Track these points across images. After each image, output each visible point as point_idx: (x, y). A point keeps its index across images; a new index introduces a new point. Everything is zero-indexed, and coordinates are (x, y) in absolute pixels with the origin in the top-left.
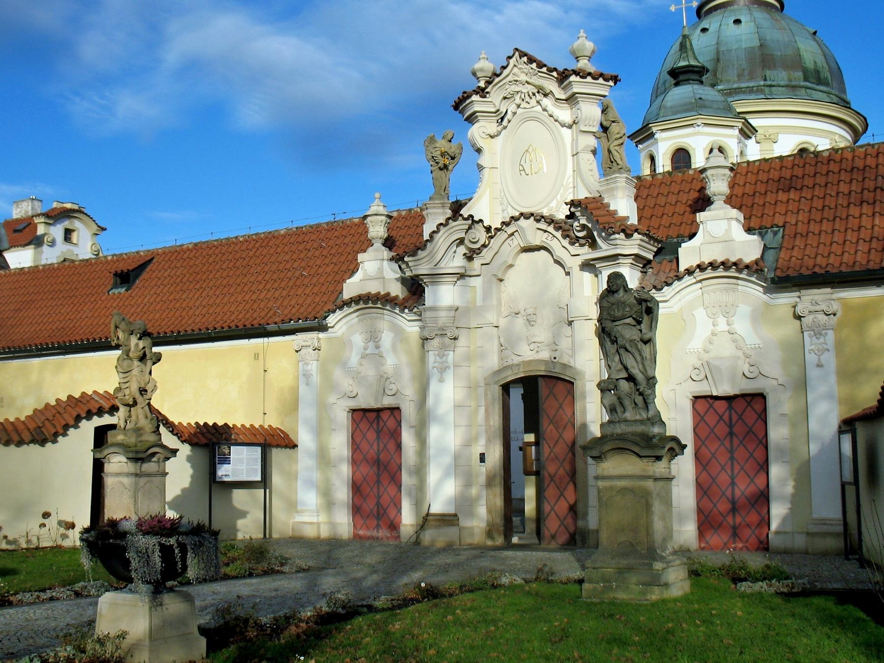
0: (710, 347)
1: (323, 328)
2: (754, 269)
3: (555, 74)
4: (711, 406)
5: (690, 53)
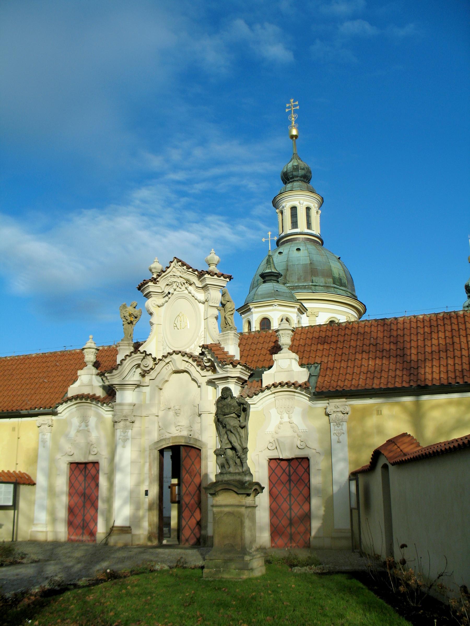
1: (55, 414)
2: (304, 387)
3: (196, 273)
4: (279, 464)
5: (272, 265)
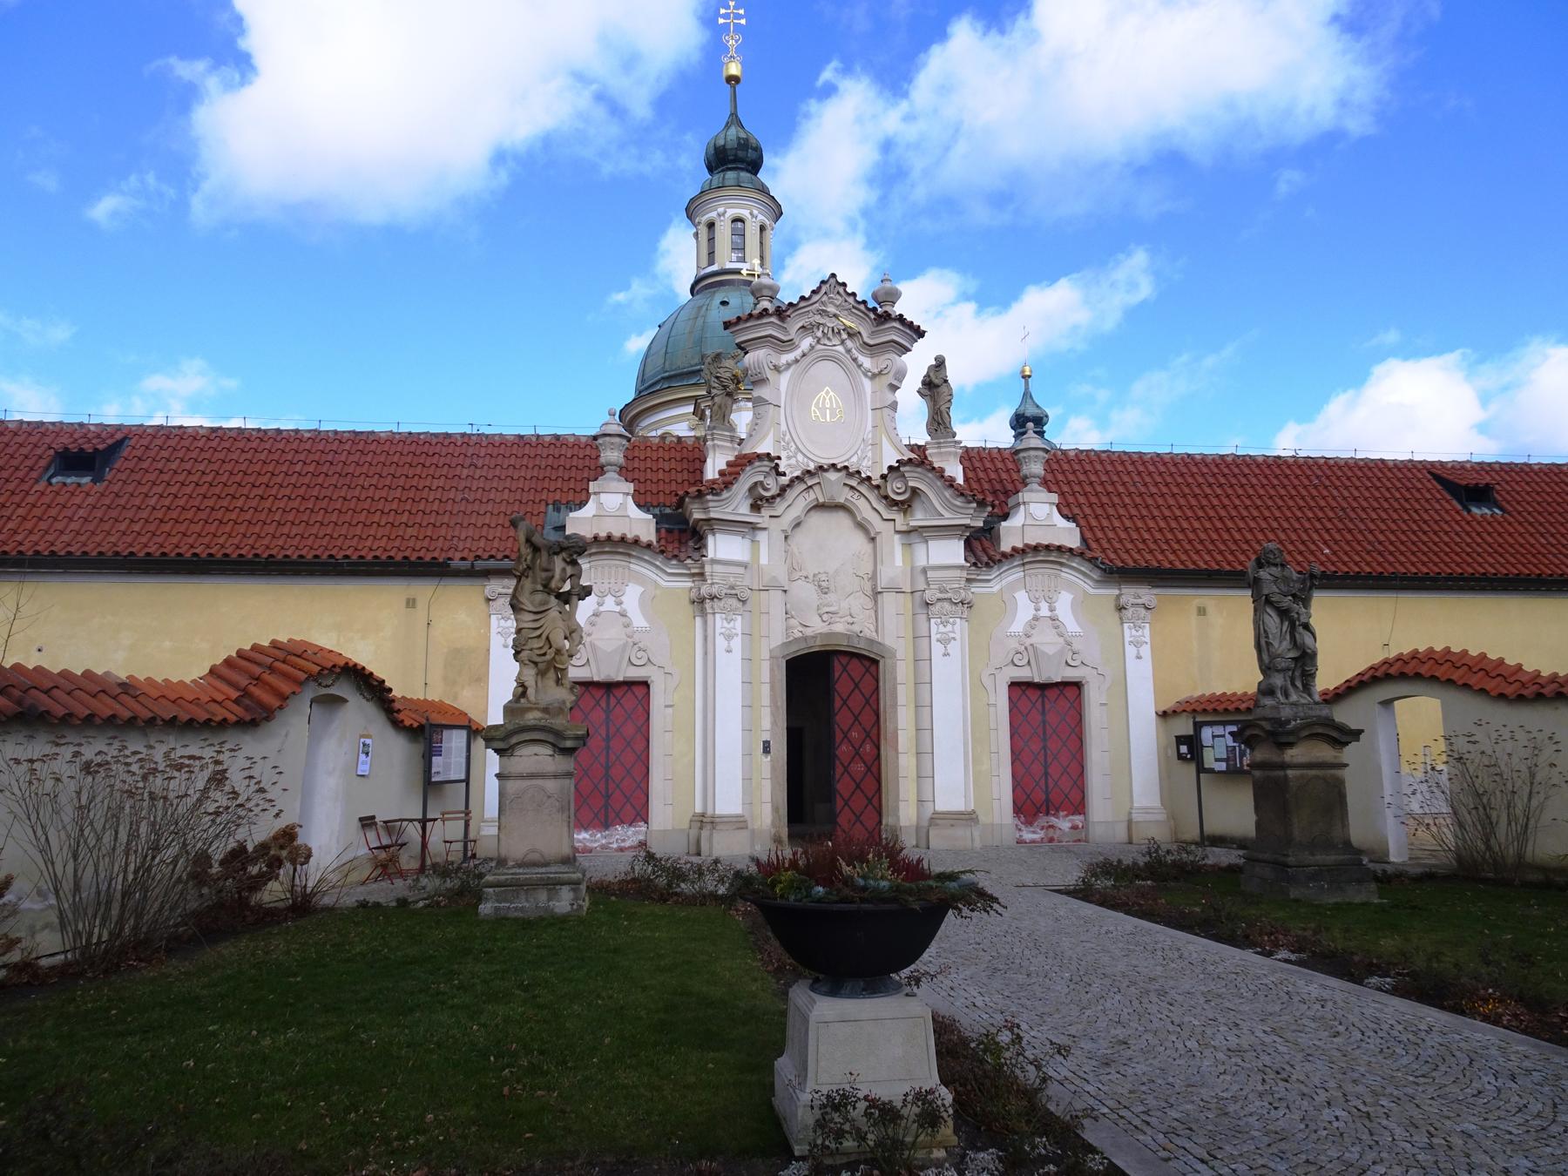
0: (1033, 632)
